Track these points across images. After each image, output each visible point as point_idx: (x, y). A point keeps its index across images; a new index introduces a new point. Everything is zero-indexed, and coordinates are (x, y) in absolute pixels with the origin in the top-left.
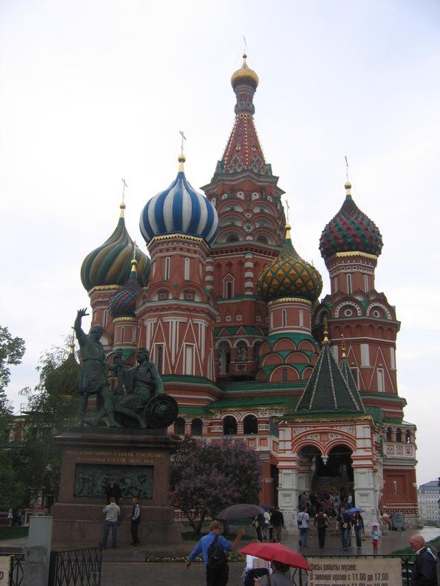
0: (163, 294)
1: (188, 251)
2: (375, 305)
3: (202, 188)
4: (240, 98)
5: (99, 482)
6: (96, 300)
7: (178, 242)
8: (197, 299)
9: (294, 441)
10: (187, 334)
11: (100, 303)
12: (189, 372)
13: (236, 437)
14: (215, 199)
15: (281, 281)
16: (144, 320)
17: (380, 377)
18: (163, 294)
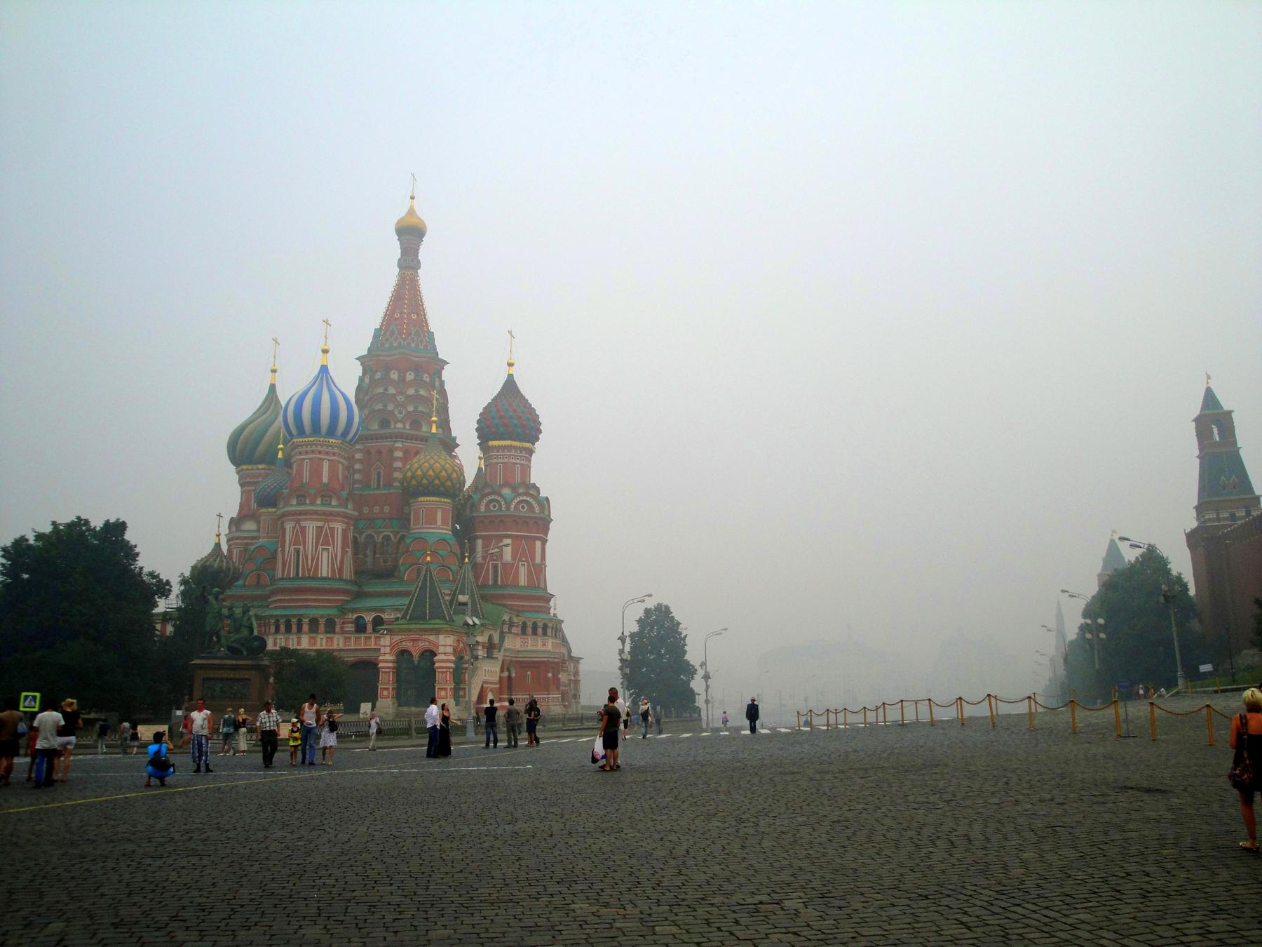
0: (302, 498)
1: (327, 453)
2: (521, 498)
3: (356, 359)
4: (405, 251)
5: (218, 689)
6: (244, 480)
7: (316, 445)
8: (334, 502)
9: (392, 647)
10: (324, 538)
11: (249, 484)
12: (324, 575)
13: (365, 635)
14: (368, 376)
15: (419, 481)
16: (283, 523)
17: (523, 572)
18: (302, 498)
